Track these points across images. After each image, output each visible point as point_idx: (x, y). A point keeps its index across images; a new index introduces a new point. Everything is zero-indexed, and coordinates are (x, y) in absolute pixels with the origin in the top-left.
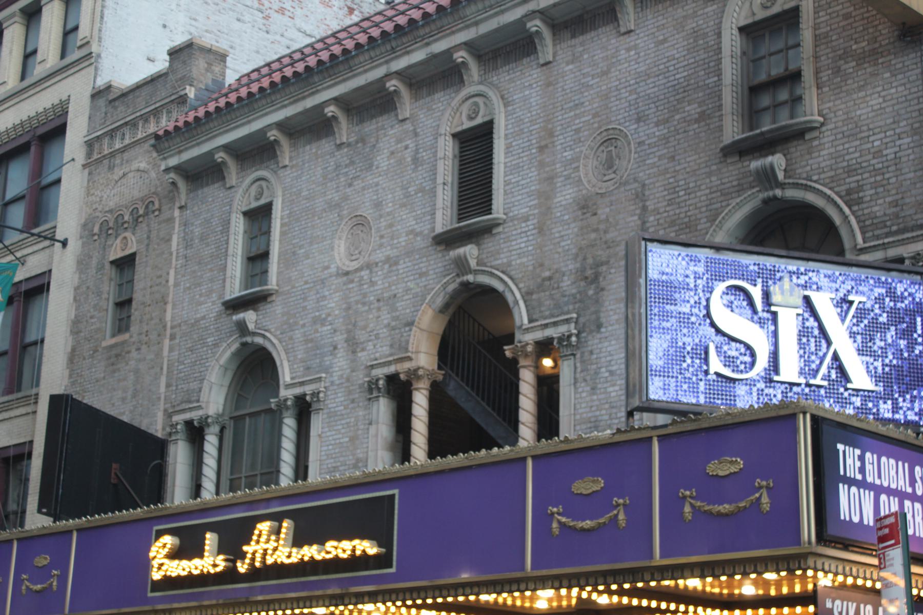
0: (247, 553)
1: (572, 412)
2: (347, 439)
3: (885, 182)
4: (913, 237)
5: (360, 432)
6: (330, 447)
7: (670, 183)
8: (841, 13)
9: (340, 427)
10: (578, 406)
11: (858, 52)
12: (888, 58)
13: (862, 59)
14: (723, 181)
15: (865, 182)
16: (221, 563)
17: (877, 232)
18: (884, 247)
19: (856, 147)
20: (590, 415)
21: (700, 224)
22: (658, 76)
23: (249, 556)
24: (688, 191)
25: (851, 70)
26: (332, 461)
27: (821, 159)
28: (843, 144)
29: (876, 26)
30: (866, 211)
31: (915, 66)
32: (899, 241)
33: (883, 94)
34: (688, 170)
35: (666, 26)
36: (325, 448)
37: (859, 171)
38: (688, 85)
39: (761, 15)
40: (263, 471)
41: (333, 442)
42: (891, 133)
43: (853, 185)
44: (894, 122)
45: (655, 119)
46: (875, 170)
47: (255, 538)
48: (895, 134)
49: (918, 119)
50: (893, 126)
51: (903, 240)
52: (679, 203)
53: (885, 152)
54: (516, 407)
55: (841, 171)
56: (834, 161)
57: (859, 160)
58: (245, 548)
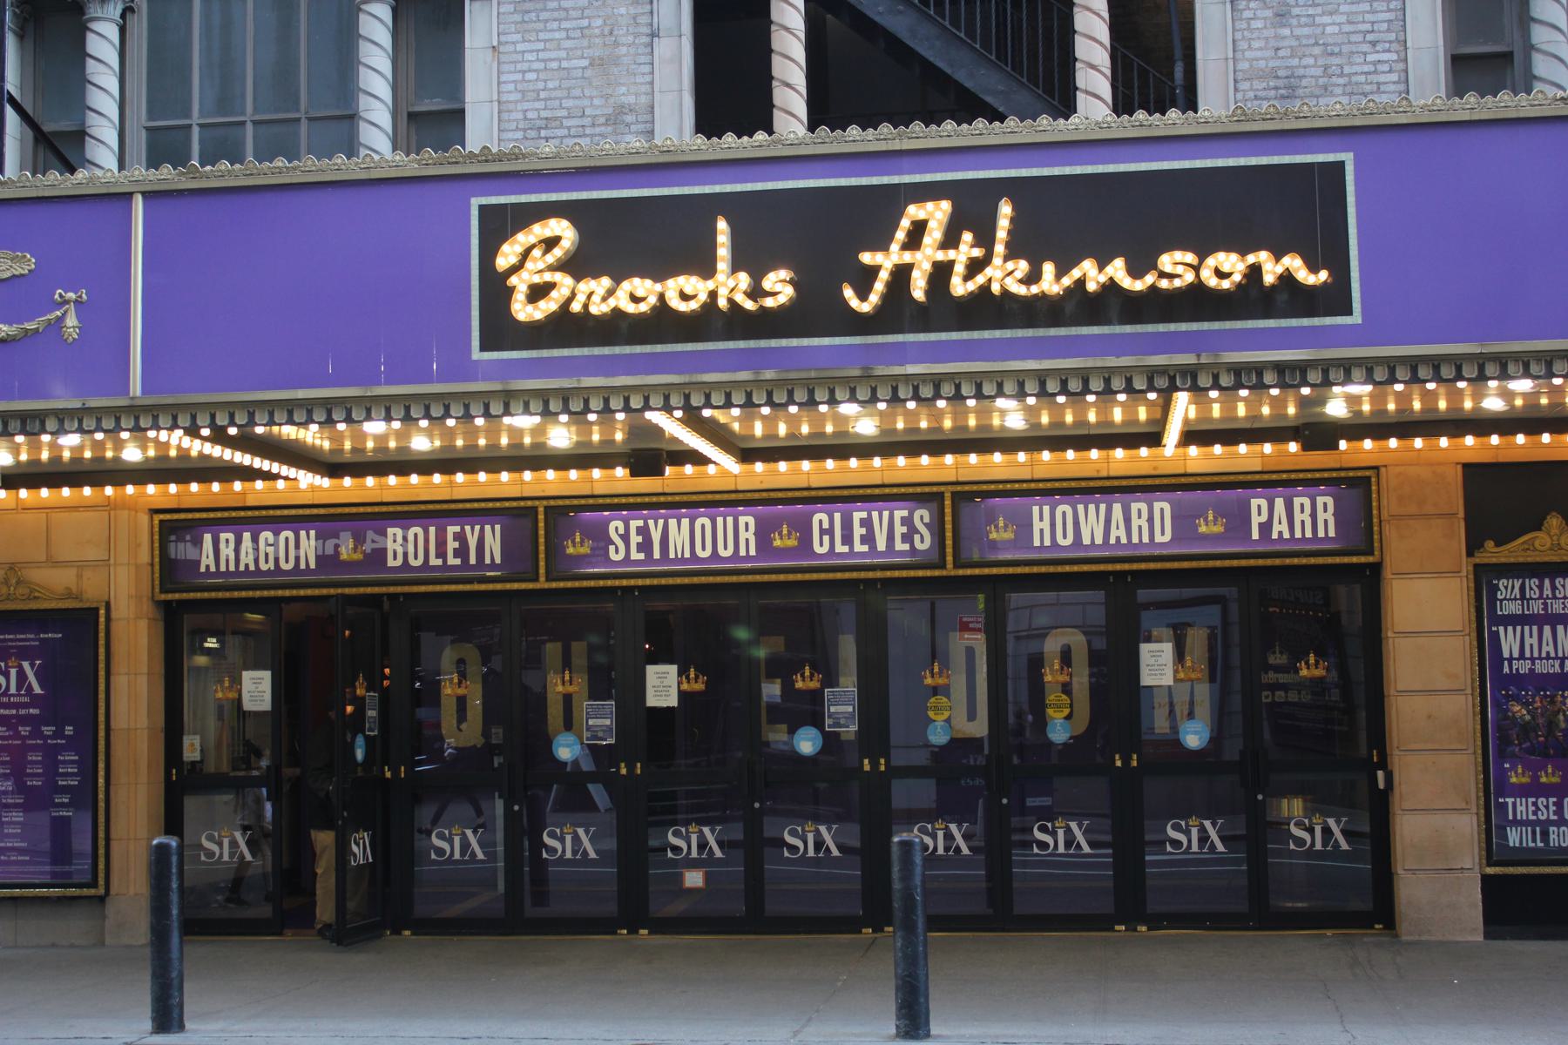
0: (874, 271)
1: (1230, 55)
2: (585, 63)
5: (624, 50)
6: (531, 76)
9: (557, 35)
10: (1243, 45)
16: (780, 287)
20: (1272, 64)
23: (884, 275)
26: (540, 105)
36: (519, 77)
40: (257, 118)
41: (541, 66)
47: (900, 235)
54: (1067, 32)
58: (866, 258)
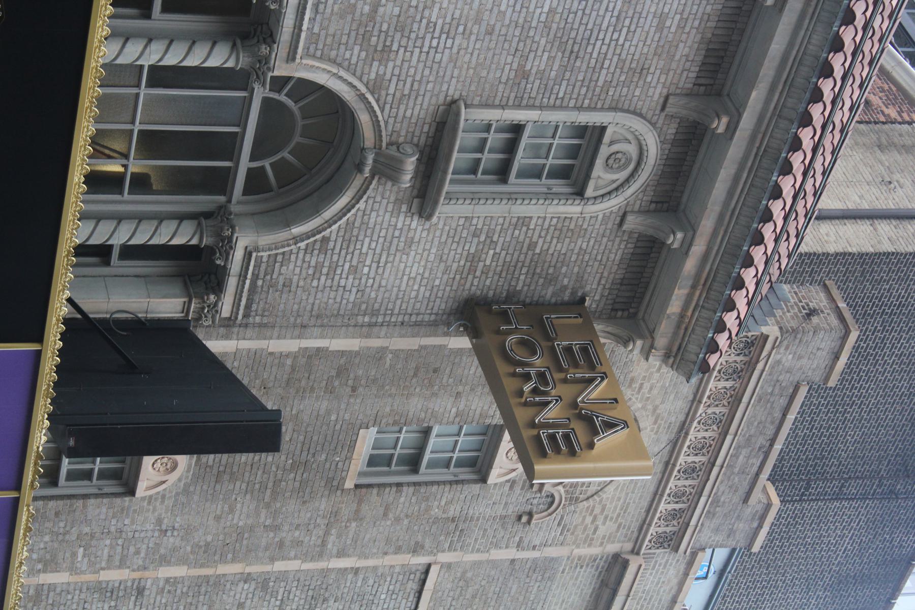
3: (317, 275)
4: (239, 305)
7: (458, 25)
8: (541, 241)
11: (484, 256)
12: (456, 283)
13: (473, 259)
14: (420, 98)
15: (328, 256)
17: (263, 266)
18: (242, 276)
19: (375, 250)
21: (380, 64)
22: (618, 18)
24: (432, 51)
25: (466, 248)
27: (381, 213)
28: (385, 237)
29: (500, 275)
30: (293, 257)
31: (430, 307)
32: (242, 292)
33: (419, 277)
34: (462, 52)
35: (680, 31)
37: (344, 252)
38: (577, 57)
39: (604, 151)
42: (369, 284)
43: (331, 244)
44: (380, 286)
45: (560, 10)
46: (337, 266)
48: (366, 286)
49: (370, 307)
50: (376, 286)
51: (241, 296)
52: (424, 38)
53: (351, 277)
55: (355, 233)
56: (371, 225)
57: (357, 252)
